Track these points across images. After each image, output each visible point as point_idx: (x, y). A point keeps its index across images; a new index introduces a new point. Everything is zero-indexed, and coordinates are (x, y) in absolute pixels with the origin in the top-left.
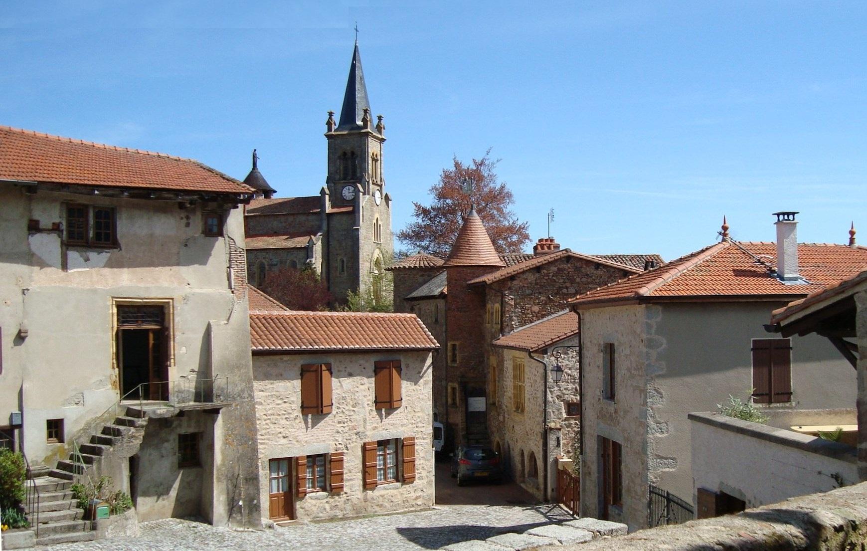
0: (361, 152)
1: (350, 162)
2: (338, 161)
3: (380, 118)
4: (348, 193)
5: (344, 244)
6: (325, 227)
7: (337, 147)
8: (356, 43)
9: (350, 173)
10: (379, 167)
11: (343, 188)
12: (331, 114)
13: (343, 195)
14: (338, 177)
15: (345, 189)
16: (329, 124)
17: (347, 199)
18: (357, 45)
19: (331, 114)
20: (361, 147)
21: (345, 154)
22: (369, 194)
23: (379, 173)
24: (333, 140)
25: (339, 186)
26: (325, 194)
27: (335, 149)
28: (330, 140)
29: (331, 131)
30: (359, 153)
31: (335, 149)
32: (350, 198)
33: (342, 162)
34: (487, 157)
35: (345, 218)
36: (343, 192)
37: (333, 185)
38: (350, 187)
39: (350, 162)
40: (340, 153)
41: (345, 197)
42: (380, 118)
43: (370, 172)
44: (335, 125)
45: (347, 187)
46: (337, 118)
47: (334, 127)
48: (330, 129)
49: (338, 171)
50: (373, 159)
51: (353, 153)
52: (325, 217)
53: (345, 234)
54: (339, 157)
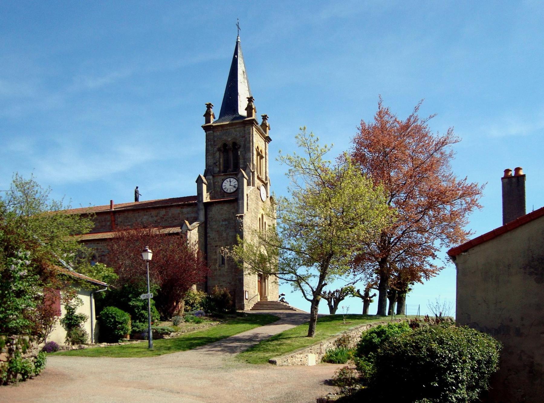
0: (245, 141)
1: (231, 155)
2: (218, 153)
3: (265, 118)
4: (229, 185)
5: (224, 235)
6: (202, 217)
7: (216, 139)
8: (237, 39)
9: (232, 166)
10: (264, 165)
11: (223, 180)
12: (209, 106)
13: (224, 187)
14: (218, 169)
15: (225, 182)
16: (207, 115)
17: (229, 191)
18: (239, 40)
19: (209, 106)
20: (244, 137)
21: (225, 145)
22: (253, 185)
23: (264, 172)
24: (211, 132)
25: (219, 179)
26: (203, 182)
27: (214, 141)
28: (208, 132)
29: (210, 122)
30: (242, 143)
31: (214, 141)
32: (232, 191)
33: (222, 154)
34: (432, 135)
35: (226, 207)
36: (224, 184)
37: (211, 177)
38: (232, 179)
39: (231, 155)
40: (219, 145)
41: (225, 190)
42: (265, 118)
43: (255, 162)
44: (214, 118)
45: (228, 180)
46: (216, 111)
47: (212, 120)
48: (208, 121)
49: (218, 164)
50: (258, 154)
51: (235, 144)
52: (202, 207)
53: (226, 225)
54: (219, 150)
